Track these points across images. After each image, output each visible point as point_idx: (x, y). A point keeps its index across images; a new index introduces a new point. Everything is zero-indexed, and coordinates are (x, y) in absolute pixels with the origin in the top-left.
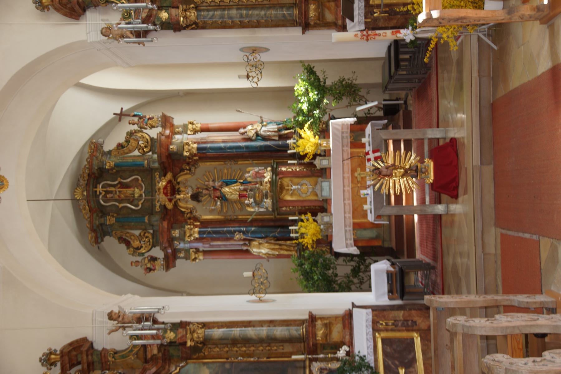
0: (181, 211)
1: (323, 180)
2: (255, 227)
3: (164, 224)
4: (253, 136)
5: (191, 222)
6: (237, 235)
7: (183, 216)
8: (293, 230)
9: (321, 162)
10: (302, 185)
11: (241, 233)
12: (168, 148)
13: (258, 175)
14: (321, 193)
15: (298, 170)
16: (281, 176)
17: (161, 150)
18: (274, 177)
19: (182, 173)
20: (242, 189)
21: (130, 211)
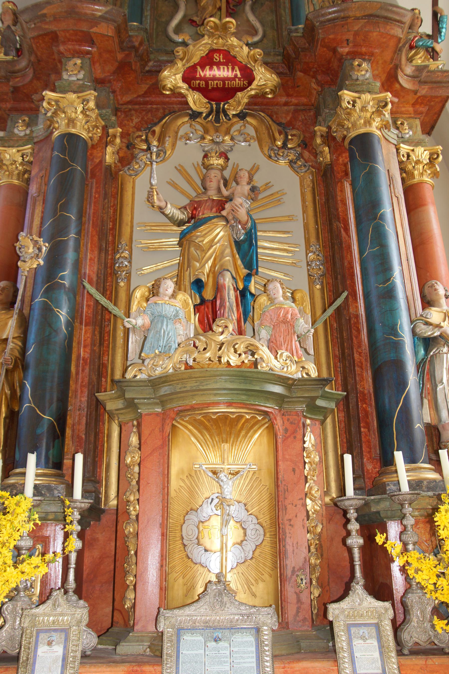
0: (156, 124)
1: (267, 635)
2: (70, 325)
3: (104, 25)
4: (427, 324)
5: (115, 136)
6: (36, 243)
7: (139, 130)
8: (24, 474)
9: (362, 630)
10: (240, 523)
11: (42, 263)
12: (361, 56)
13: (283, 327)
14: (193, 629)
15: (308, 502)
16: (279, 423)
17: (357, 19)
18: (277, 389)
19: (275, 127)
20: (221, 281)
21: (164, 20)
